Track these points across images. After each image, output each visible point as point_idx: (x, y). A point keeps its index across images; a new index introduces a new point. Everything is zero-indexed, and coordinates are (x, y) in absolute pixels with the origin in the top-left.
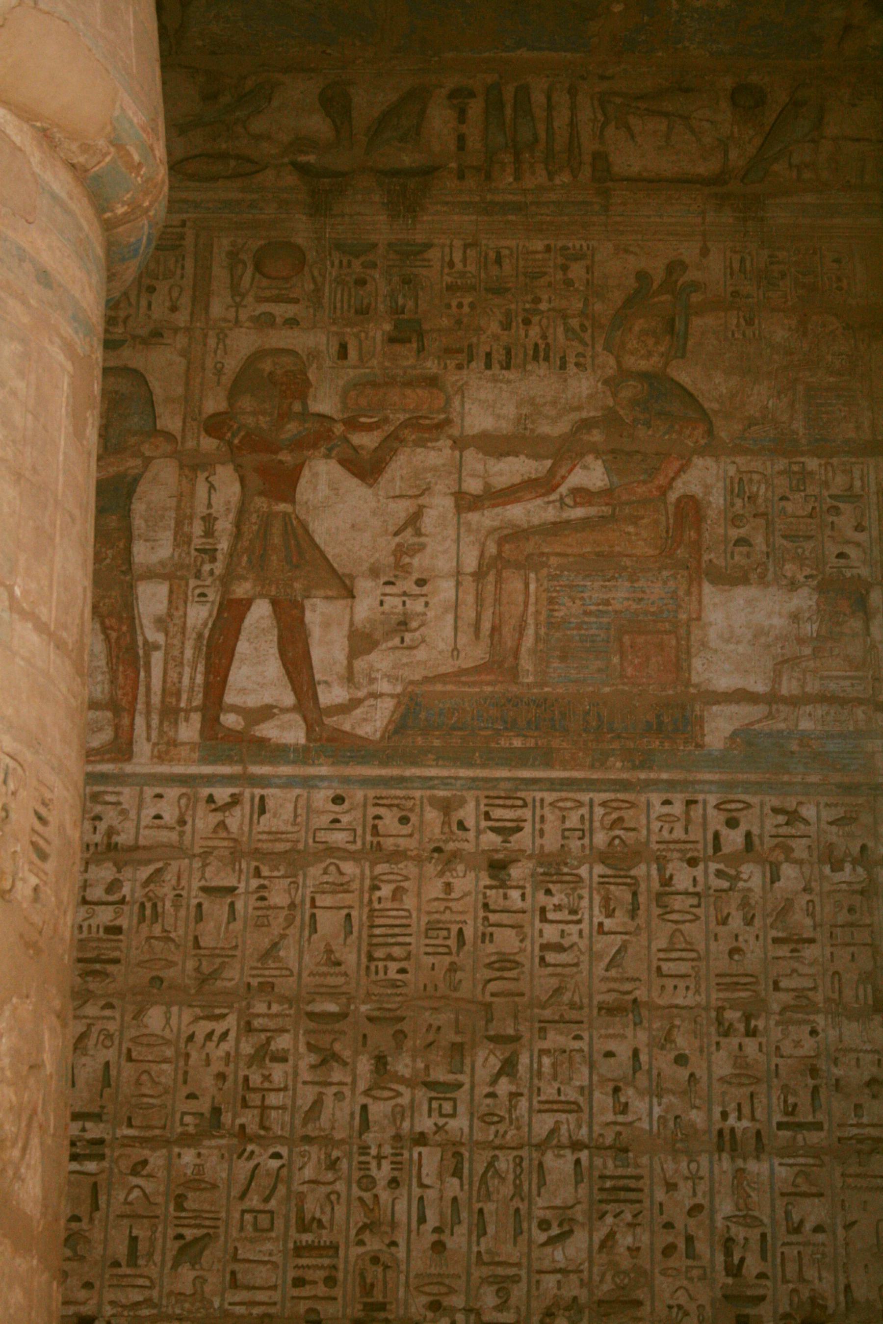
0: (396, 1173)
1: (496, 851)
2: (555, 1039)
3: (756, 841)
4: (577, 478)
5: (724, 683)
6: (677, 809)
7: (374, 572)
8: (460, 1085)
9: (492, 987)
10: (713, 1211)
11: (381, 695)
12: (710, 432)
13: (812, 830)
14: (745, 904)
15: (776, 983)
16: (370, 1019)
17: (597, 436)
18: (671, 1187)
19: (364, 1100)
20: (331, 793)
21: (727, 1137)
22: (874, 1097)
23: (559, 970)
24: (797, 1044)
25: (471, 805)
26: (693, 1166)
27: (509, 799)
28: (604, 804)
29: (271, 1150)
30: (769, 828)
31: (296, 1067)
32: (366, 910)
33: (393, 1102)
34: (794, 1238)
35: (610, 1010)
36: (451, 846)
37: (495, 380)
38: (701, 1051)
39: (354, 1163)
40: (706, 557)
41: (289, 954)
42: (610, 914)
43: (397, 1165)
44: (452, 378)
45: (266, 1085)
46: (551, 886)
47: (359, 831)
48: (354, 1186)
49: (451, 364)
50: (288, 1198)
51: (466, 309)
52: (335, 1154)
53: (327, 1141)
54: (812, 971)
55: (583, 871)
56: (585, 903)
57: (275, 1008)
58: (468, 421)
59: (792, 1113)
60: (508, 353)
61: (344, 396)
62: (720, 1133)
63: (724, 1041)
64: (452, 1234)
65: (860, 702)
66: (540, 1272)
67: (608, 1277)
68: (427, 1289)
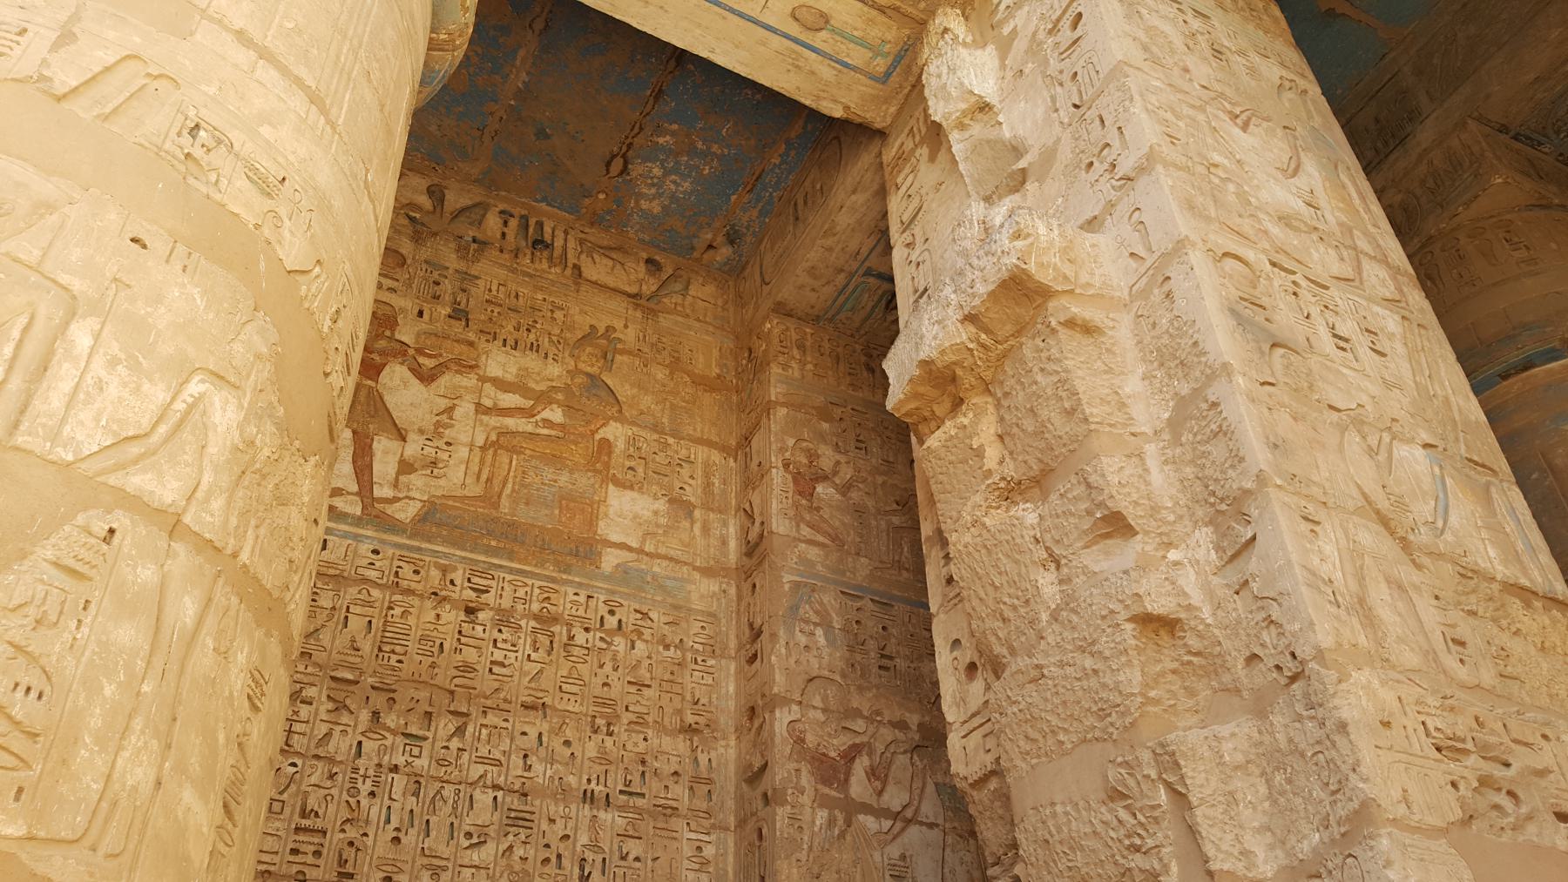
0: (375, 789)
1: (471, 601)
2: (492, 719)
3: (624, 625)
4: (546, 414)
5: (615, 537)
6: (582, 599)
7: (421, 432)
8: (425, 739)
9: (457, 681)
10: (575, 840)
11: (414, 499)
12: (620, 411)
13: (655, 625)
14: (614, 659)
15: (627, 707)
16: (373, 688)
17: (560, 396)
18: (552, 821)
19: (361, 738)
20: (372, 547)
21: (589, 795)
22: (676, 783)
23: (500, 678)
24: (636, 744)
25: (460, 572)
26: (567, 810)
27: (483, 574)
28: (540, 588)
29: (291, 761)
30: (632, 620)
31: (317, 710)
32: (383, 620)
33: (380, 742)
34: (623, 863)
35: (525, 706)
36: (443, 593)
37: (507, 353)
38: (580, 740)
39: (347, 778)
40: (612, 471)
41: (325, 637)
42: (536, 650)
43: (376, 783)
44: (482, 345)
45: (295, 718)
46: (502, 628)
47: (387, 573)
48: (345, 792)
49: (483, 338)
50: (297, 794)
51: (495, 314)
52: (334, 771)
53: (331, 760)
54: (648, 704)
55: (523, 623)
56: (521, 641)
57: (310, 670)
58: (488, 369)
59: (628, 786)
60: (516, 343)
61: (418, 335)
62: (585, 791)
63: (593, 736)
64: (406, 834)
65: (686, 564)
66: (461, 866)
67: (505, 875)
68: (384, 868)
